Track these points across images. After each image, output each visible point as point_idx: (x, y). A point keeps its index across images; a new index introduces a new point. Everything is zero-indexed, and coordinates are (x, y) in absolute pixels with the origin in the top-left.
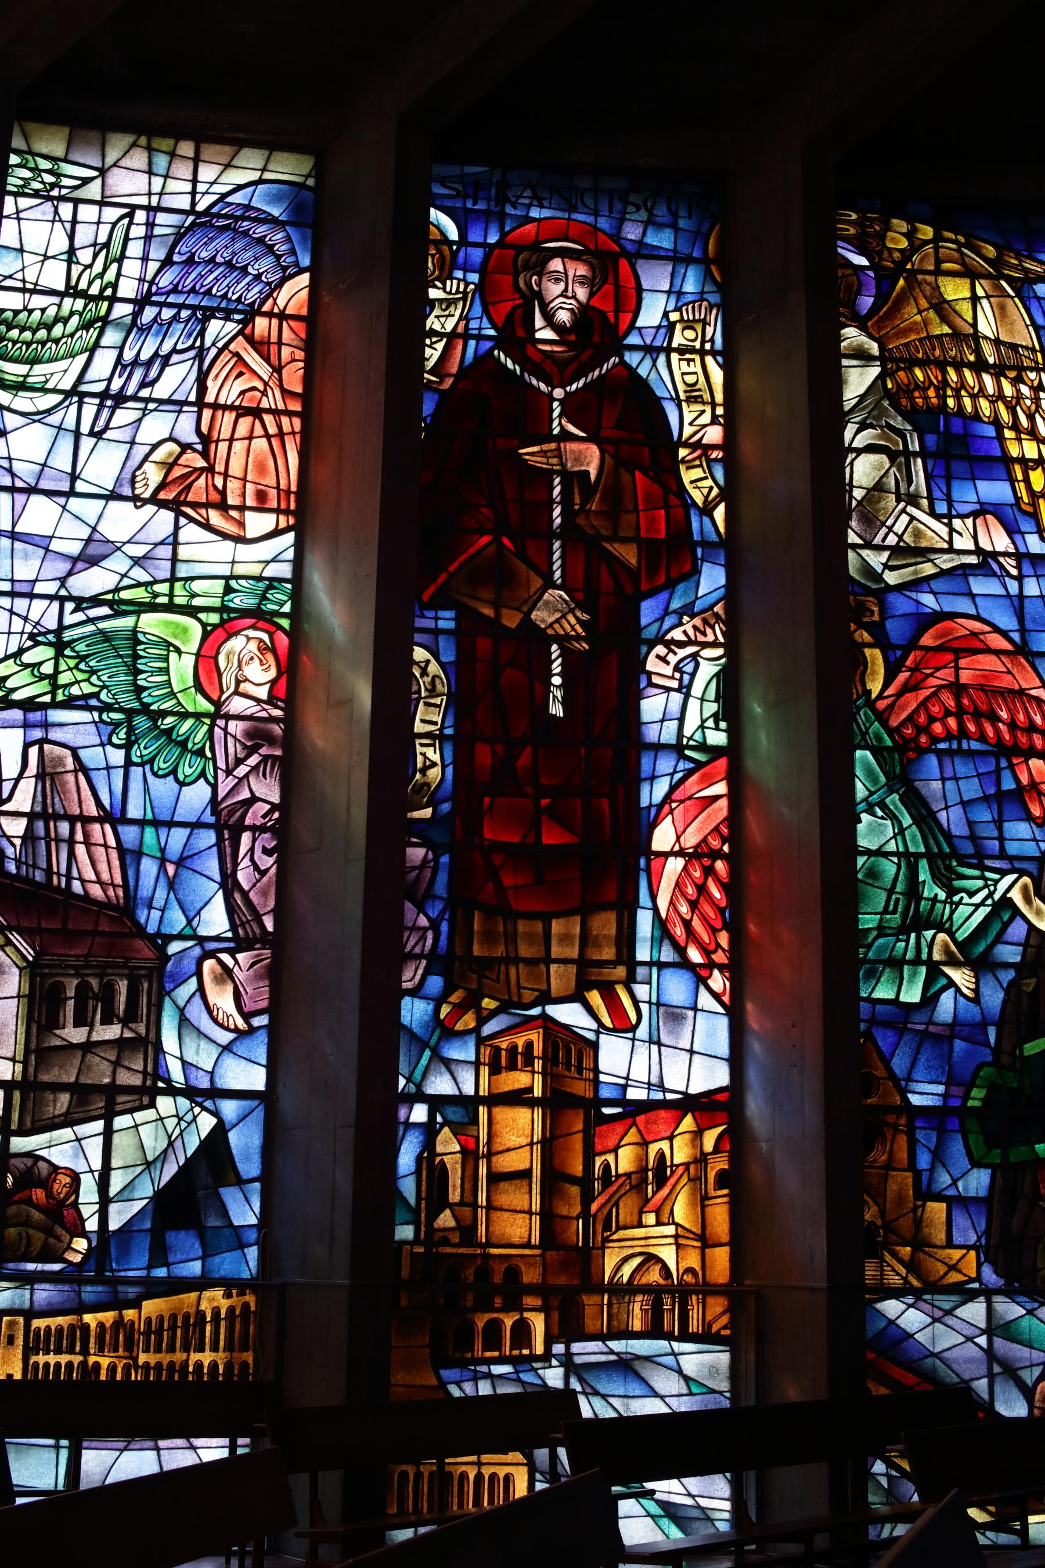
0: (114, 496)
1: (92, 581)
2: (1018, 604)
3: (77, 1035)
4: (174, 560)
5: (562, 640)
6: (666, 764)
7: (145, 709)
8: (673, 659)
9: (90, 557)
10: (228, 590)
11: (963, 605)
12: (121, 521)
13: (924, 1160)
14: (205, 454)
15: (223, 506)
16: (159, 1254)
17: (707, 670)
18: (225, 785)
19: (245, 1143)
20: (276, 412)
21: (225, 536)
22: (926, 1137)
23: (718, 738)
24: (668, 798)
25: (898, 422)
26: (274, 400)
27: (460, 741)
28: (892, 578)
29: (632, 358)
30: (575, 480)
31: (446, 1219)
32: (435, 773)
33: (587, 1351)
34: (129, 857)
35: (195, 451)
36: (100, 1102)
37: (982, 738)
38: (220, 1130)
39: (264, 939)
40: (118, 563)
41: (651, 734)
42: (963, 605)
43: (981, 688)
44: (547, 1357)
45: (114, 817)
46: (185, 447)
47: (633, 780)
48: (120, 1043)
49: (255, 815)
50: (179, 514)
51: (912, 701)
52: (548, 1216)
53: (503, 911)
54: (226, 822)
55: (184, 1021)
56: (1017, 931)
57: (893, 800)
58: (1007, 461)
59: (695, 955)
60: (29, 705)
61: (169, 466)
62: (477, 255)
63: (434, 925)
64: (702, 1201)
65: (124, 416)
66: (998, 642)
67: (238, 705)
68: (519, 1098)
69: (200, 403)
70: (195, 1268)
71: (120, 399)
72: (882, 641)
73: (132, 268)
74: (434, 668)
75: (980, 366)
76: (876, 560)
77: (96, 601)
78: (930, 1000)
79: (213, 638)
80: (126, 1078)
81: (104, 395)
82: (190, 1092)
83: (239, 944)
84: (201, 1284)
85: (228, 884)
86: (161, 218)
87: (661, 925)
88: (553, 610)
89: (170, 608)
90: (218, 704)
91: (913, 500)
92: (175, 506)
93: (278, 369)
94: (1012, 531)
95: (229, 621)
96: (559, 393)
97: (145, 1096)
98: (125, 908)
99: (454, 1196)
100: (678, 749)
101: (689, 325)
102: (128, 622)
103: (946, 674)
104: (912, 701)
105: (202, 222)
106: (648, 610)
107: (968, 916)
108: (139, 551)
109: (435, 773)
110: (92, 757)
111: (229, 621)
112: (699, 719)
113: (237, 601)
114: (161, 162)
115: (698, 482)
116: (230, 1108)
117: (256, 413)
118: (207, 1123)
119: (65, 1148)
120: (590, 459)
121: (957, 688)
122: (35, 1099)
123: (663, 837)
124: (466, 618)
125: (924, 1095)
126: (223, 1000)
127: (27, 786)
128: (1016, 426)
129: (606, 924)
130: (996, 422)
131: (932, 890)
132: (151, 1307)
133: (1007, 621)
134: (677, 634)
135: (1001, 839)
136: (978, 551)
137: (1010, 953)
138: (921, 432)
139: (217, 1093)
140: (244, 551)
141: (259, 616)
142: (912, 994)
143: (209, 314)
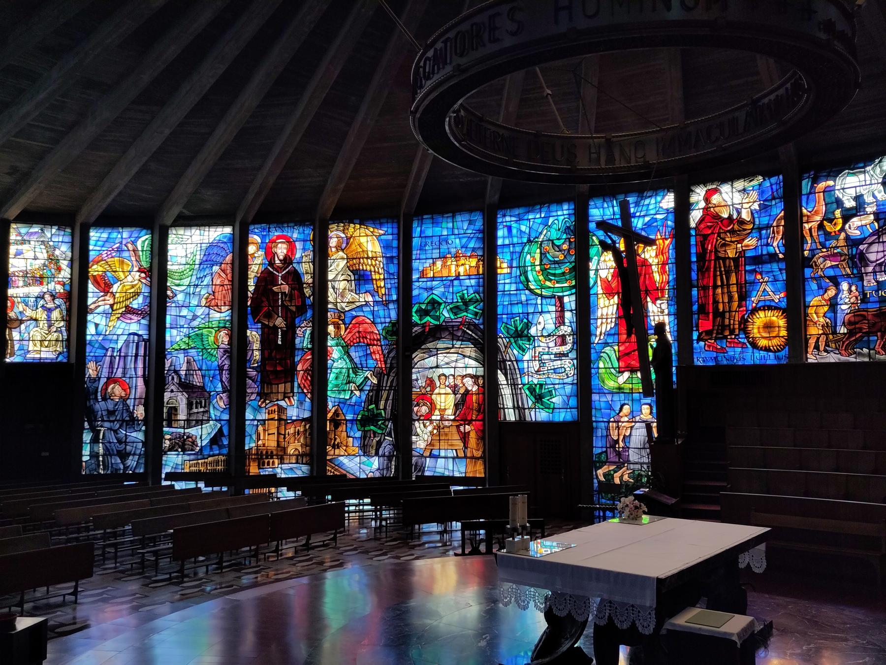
1: (195, 323)
2: (373, 312)
3: (195, 410)
9: (195, 317)
11: (361, 314)
15: (217, 306)
16: (211, 449)
17: (308, 332)
18: (220, 362)
19: (225, 431)
23: (309, 346)
25: (350, 273)
27: (262, 350)
28: (347, 309)
29: (295, 265)
30: (283, 294)
31: (260, 442)
34: (203, 376)
36: (199, 422)
38: (221, 427)
39: (228, 391)
41: (297, 347)
42: (361, 314)
45: (200, 370)
48: (203, 412)
49: (226, 367)
51: (350, 335)
52: (278, 441)
53: (270, 384)
54: (221, 368)
55: (214, 407)
56: (369, 383)
57: (345, 357)
58: (372, 279)
59: (305, 391)
60: (184, 349)
61: (207, 299)
64: (305, 438)
66: (368, 321)
67: (222, 346)
68: (272, 419)
70: (217, 452)
72: (344, 324)
75: (368, 258)
76: (344, 305)
80: (205, 418)
82: (216, 420)
83: (224, 392)
84: (219, 455)
85: (221, 381)
88: (280, 322)
91: (352, 291)
92: (209, 307)
95: (220, 329)
97: (208, 421)
98: (203, 388)
100: (303, 349)
103: (357, 329)
104: (350, 335)
106: (297, 321)
110: (196, 358)
111: (220, 329)
112: (306, 344)
113: (221, 325)
115: (308, 292)
116: (223, 422)
118: (219, 425)
120: (286, 288)
121: (359, 332)
122: (189, 423)
123: (299, 368)
124: (263, 324)
126: (222, 404)
127: (185, 364)
129: (289, 385)
130: (371, 271)
131: (352, 375)
132: (210, 459)
133: (371, 317)
139: (220, 420)
140: (222, 315)
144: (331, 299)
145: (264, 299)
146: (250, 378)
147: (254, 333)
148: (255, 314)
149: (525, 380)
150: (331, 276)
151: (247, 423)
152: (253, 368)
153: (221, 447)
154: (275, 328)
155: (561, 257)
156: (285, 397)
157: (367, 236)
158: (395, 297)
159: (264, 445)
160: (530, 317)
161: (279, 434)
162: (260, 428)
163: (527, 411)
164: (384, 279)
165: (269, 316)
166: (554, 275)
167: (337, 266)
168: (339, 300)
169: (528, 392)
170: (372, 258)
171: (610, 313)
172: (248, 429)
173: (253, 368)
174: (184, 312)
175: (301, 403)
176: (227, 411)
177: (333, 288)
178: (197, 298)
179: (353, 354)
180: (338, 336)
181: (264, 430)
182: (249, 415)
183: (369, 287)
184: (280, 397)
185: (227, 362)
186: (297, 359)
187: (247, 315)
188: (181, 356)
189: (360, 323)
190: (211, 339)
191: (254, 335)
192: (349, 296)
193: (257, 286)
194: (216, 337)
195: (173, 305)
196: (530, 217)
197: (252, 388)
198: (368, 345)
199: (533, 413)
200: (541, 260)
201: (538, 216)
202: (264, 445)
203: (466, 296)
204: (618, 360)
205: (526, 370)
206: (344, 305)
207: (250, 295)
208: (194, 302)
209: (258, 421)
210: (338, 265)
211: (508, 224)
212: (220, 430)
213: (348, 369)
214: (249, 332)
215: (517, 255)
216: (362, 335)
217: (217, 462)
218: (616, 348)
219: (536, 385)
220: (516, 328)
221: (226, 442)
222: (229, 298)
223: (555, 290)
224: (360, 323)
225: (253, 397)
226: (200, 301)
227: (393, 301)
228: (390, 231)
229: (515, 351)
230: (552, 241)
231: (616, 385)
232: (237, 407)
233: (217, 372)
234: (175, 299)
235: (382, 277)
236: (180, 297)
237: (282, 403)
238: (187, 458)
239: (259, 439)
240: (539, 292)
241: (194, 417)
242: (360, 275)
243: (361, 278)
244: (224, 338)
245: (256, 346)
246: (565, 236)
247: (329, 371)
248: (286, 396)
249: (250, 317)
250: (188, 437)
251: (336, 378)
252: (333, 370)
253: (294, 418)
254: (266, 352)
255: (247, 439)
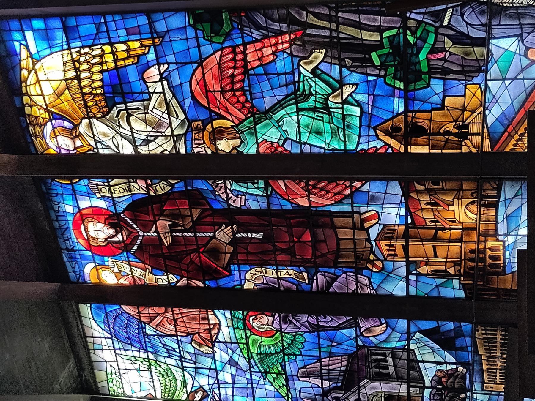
0: (214, 358)
1: (243, 363)
2: (180, 64)
3: (391, 369)
4: (231, 343)
5: (234, 234)
6: (276, 201)
7: (282, 351)
8: (234, 198)
10: (238, 328)
12: (221, 355)
13: (427, 107)
14: (194, 334)
15: (210, 330)
16: (463, 349)
17: (235, 186)
18: (303, 329)
20: (173, 315)
21: (219, 329)
22: (417, 105)
23: (261, 184)
24: (288, 200)
26: (169, 315)
28: (182, 116)
31: (451, 271)
32: (290, 272)
33: (502, 229)
34: (331, 355)
35: (193, 337)
36: (413, 363)
37: (243, 81)
38: (421, 332)
39: (355, 318)
40: (236, 357)
41: (264, 205)
43: (221, 81)
44: (504, 241)
45: (319, 359)
46: (192, 340)
47: (282, 213)
48: (394, 358)
50: (215, 341)
51: (232, 109)
52: (450, 241)
53: (338, 252)
54: (316, 329)
55: (385, 341)
57: (276, 117)
58: (117, 68)
59: (348, 191)
60: (287, 380)
61: (200, 345)
62: (97, 258)
63: (345, 272)
64: (444, 191)
65: (187, 356)
66: (199, 72)
67: (276, 325)
68: (406, 249)
69: (176, 336)
70: (468, 339)
71: (181, 357)
72: (211, 120)
73: (136, 354)
74: (253, 271)
76: (175, 123)
77: (250, 363)
78: (358, 104)
79: (253, 331)
81: (181, 361)
82: (409, 340)
83: (357, 326)
86: (116, 346)
87: (337, 203)
88: (224, 235)
89: (247, 343)
90: (277, 331)
91: (146, 108)
92: (213, 343)
93: (158, 314)
94: (148, 66)
95: (247, 327)
96: (141, 233)
99: (443, 268)
100: (268, 197)
101: (100, 191)
102: (255, 356)
103: (219, 96)
104: (232, 109)
105: (114, 335)
107: (321, 88)
108: (230, 352)
109: (290, 272)
111: (247, 327)
112: (255, 189)
113: (241, 325)
114: (96, 346)
115: (162, 188)
116: (413, 329)
117: (175, 321)
118: (418, 335)
119: (429, 373)
120: (163, 224)
121: (223, 91)
123: (303, 202)
125: (399, 105)
127: (312, 380)
128: (101, 64)
129: (338, 221)
130: (102, 72)
133: (189, 69)
134: (224, 196)
135: (285, 74)
136: (161, 80)
137: (336, 71)
138: (115, 104)
139: (408, 332)
140: (223, 322)
141: (245, 320)
142: (357, 111)
143: (145, 334)
144: (169, 146)
145: (187, 260)
146: (329, 284)
147: (248, 276)
148: (215, 275)
150: (127, 149)
151: (413, 291)
152: (311, 279)
153: (458, 333)
154: (234, 242)
156: (362, 228)
157: (38, 81)
158: (143, 20)
159: (456, 264)
161: (435, 238)
162: (424, 269)
164: (111, 44)
165: (216, 253)
167: (108, 137)
168: (168, 132)
170: (77, 70)
172: (426, 287)
173: (311, 279)
174: (226, 376)
175: (372, 199)
176: (393, 321)
177: (147, 142)
178: (201, 358)
179: (268, 102)
180: (236, 132)
181: (427, 263)
182: (398, 289)
183: (132, 74)
184: (362, 236)
185: (304, 318)
186: (287, 206)
187: (219, 288)
188: (298, 385)
189: (207, 92)
190: (266, 341)
191: (252, 278)
192: (158, 112)
193: (167, 271)
194: (262, 334)
195: (216, 391)
197: (346, 282)
198: (246, 72)
202: (456, 264)
206: (175, 123)
207: (183, 282)
208: (208, 362)
209: (409, 273)
210: (105, 135)
212: (426, 333)
213: (299, 110)
214: (248, 286)
216: (229, 85)
217: (487, 341)
221: (450, 325)
222: (195, 312)
224: (207, 92)
225: (364, 280)
226: (205, 354)
227: (151, 23)
228: (17, 36)
232: (386, 307)
233: (322, 334)
234: (207, 388)
235: (108, 49)
236: (204, 381)
237: (374, 233)
238: (477, 387)
239: (444, 273)
241: (404, 372)
242: (114, 93)
243: (118, 92)
244: (263, 321)
245: (271, 273)
247: (307, 149)
248: (361, 226)
249: (222, 282)
250: (439, 382)
251: (319, 133)
252: (304, 140)
253: (403, 212)
254: (280, 258)
255: (446, 293)
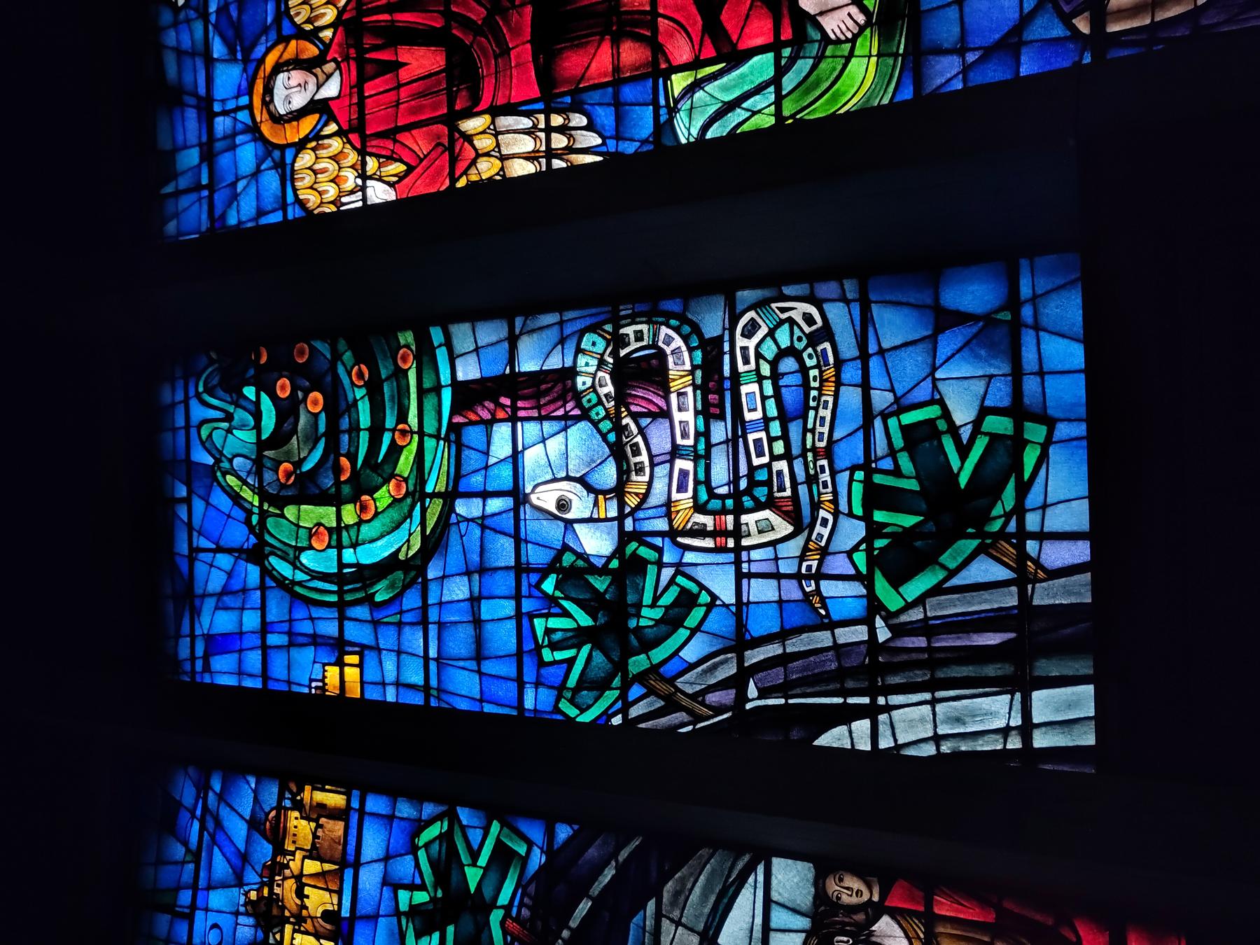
149: (843, 595)
155: (316, 400)
160: (536, 556)
163: (1043, 595)
166: (376, 431)
169: (914, 589)
171: (527, 144)
196: (183, 548)
199: (1057, 555)
200: (322, 499)
201: (183, 513)
203: (421, 897)
204: (736, 58)
205: (792, 591)
211: (200, 650)
215: (300, 613)
218: (679, 82)
219: (874, 530)
220: (579, 636)
223: (430, 427)
229: (690, 654)
230: (261, 445)
231: (869, 44)
240: (435, 508)
246: (249, 392)
